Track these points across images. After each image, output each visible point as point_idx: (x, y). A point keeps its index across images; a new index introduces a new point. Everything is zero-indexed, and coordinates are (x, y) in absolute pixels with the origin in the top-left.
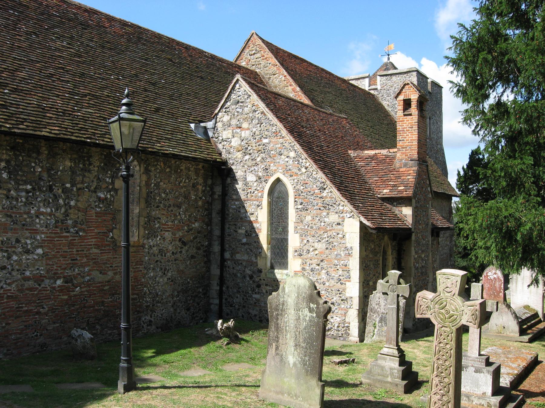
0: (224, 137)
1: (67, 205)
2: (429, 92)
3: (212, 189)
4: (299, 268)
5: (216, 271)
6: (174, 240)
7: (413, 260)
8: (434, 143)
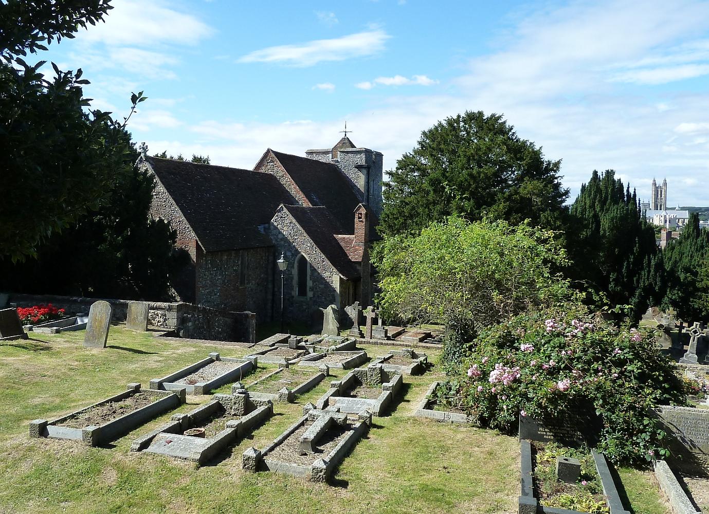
0: (274, 233)
1: (225, 274)
2: (374, 162)
3: (268, 258)
4: (312, 296)
5: (270, 297)
6: (255, 284)
7: (361, 290)
8: (376, 197)
